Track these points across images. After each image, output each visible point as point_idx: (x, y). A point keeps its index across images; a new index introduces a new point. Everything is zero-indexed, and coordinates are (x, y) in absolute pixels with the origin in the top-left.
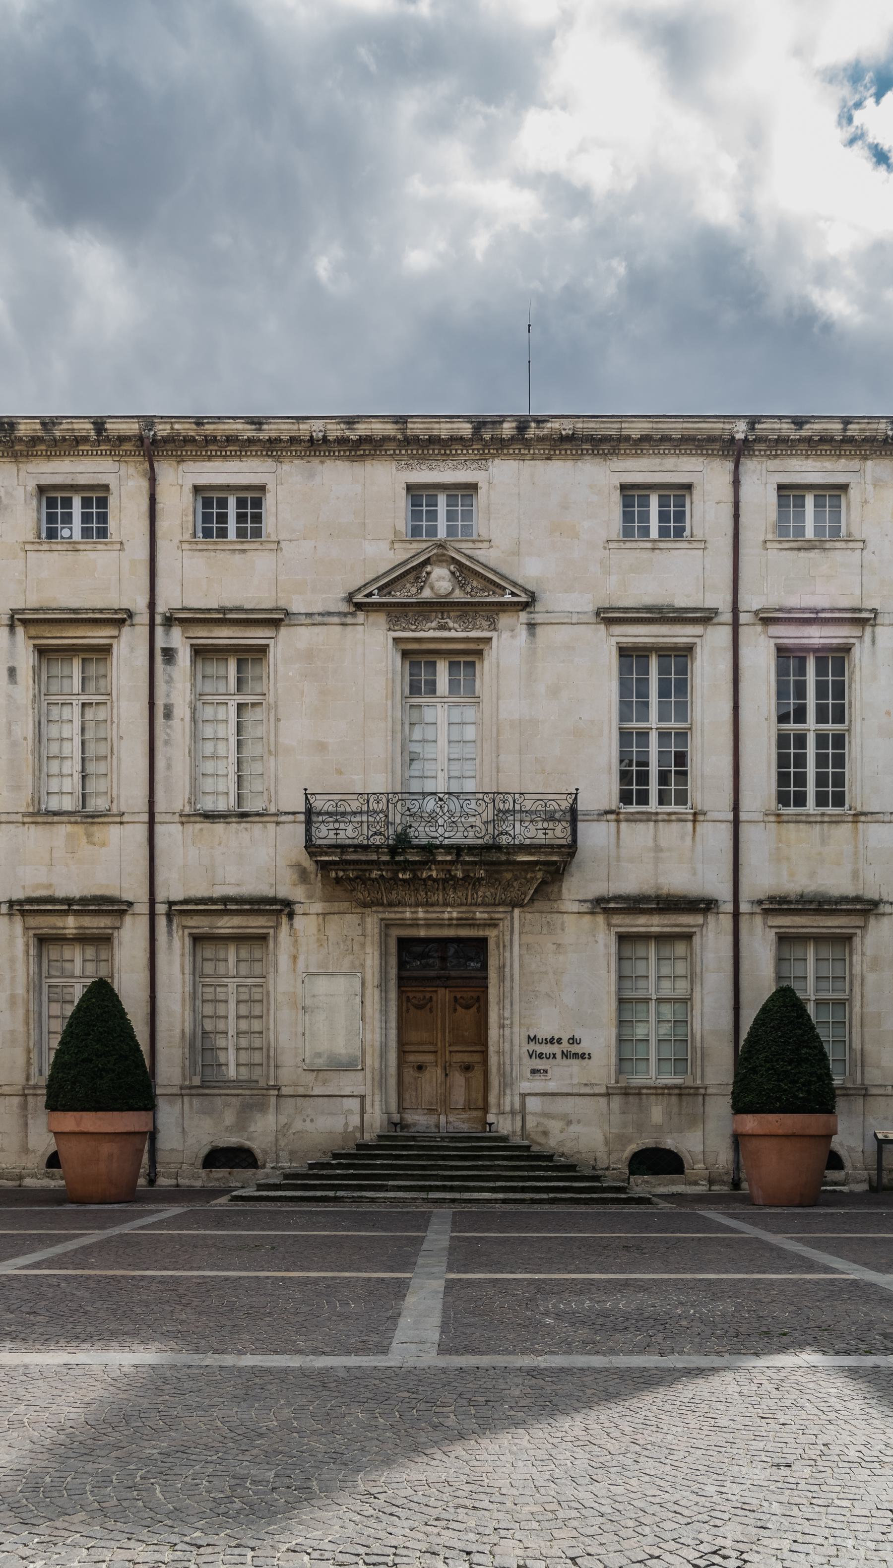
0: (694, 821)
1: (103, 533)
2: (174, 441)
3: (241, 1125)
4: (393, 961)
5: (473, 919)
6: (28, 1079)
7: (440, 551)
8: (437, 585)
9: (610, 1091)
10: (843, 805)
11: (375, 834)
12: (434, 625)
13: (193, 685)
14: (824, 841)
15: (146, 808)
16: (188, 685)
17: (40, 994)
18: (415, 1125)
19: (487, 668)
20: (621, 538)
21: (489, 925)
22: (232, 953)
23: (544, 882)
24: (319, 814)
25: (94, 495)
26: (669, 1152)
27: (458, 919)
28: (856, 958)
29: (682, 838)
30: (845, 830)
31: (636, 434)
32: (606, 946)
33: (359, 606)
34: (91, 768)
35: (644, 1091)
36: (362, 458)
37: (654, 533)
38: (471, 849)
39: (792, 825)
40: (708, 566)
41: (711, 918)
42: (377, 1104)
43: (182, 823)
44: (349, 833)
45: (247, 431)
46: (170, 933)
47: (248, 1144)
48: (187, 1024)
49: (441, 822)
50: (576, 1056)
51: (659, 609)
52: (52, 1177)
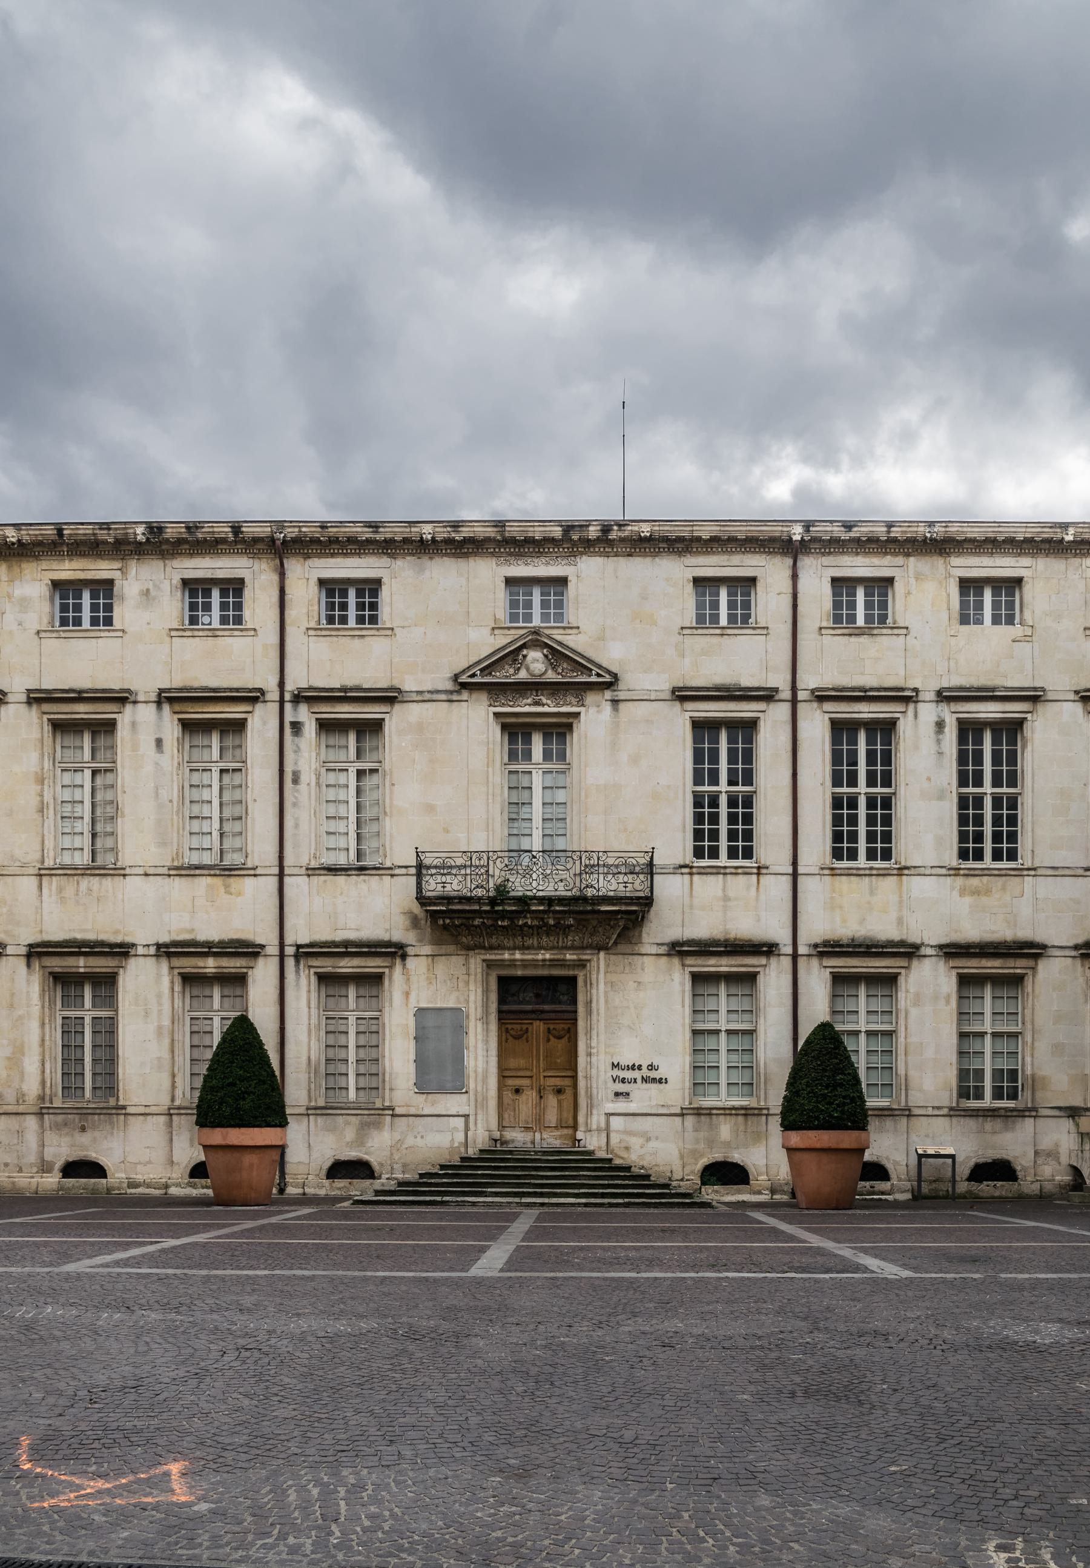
0: (758, 874)
2: (302, 541)
3: (360, 1140)
4: (494, 997)
5: (564, 960)
6: (173, 1100)
7: (534, 637)
9: (685, 1112)
10: (890, 859)
11: (477, 887)
12: (529, 701)
13: (318, 754)
14: (872, 892)
15: (276, 863)
16: (314, 754)
18: (513, 1141)
20: (694, 625)
21: (579, 966)
23: (626, 928)
24: (428, 868)
27: (550, 960)
28: (901, 995)
29: (748, 888)
30: (892, 881)
31: (705, 536)
32: (682, 984)
33: (464, 686)
34: (99, 828)
35: (714, 1112)
36: (466, 555)
37: (723, 621)
38: (561, 900)
39: (844, 878)
40: (770, 650)
41: (773, 961)
43: (309, 875)
44: (455, 885)
45: (366, 534)
46: (297, 972)
47: (366, 1157)
48: (312, 1052)
49: (534, 876)
50: (654, 1080)
51: (727, 689)
52: (194, 1186)
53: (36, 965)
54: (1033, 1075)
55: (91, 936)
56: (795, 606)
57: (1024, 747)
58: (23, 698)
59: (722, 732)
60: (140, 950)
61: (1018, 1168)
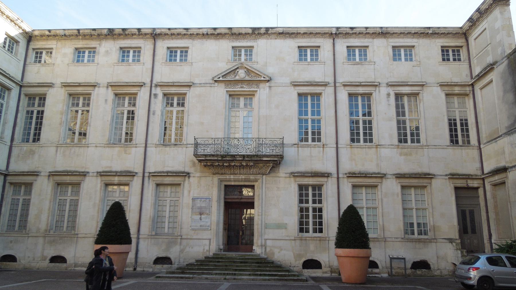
1: (139, 61)
4: (223, 193)
8: (240, 75)
12: (239, 86)
16: (161, 105)
17: (104, 203)
19: (255, 99)
22: (169, 189)
23: (273, 167)
24: (200, 144)
25: (137, 50)
26: (316, 261)
28: (379, 193)
30: (374, 150)
35: (308, 239)
37: (309, 60)
38: (248, 156)
41: (329, 179)
42: (215, 242)
44: (209, 151)
45: (185, 32)
46: (149, 183)
53: (51, 178)
54: (434, 225)
55: (73, 169)
56: (334, 55)
57: (420, 102)
58: (60, 86)
59: (308, 98)
60: (91, 174)
61: (431, 264)
